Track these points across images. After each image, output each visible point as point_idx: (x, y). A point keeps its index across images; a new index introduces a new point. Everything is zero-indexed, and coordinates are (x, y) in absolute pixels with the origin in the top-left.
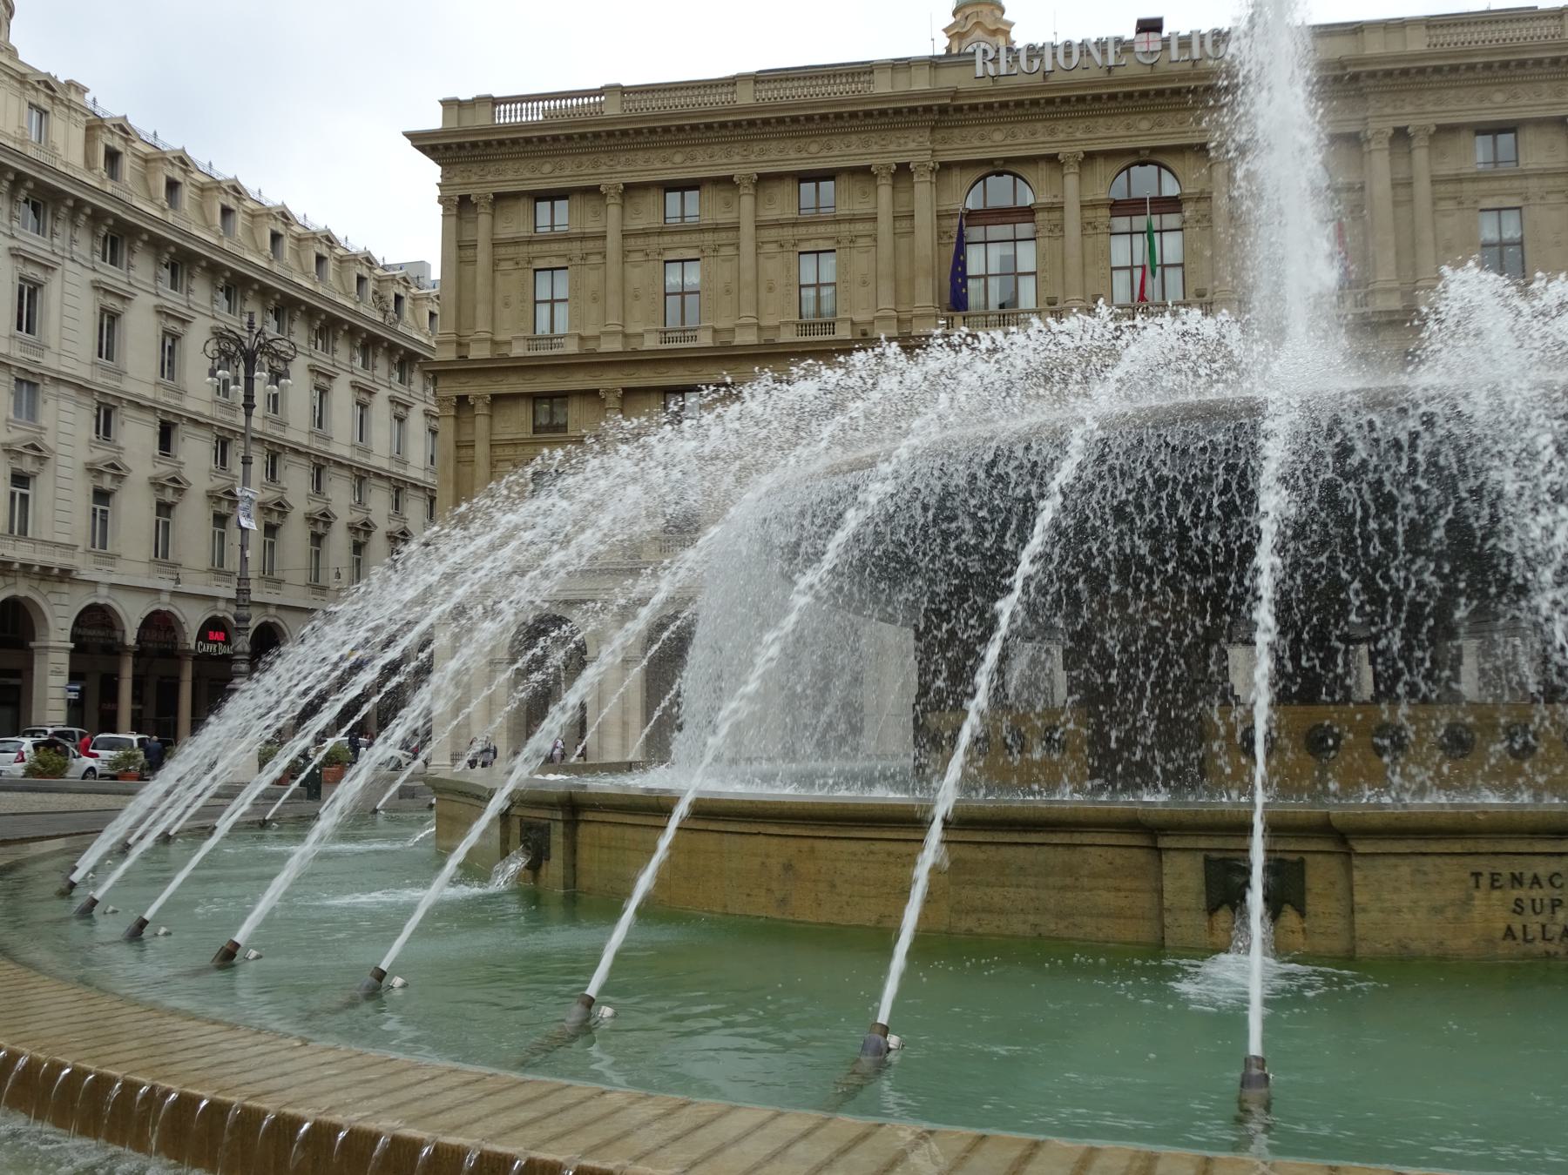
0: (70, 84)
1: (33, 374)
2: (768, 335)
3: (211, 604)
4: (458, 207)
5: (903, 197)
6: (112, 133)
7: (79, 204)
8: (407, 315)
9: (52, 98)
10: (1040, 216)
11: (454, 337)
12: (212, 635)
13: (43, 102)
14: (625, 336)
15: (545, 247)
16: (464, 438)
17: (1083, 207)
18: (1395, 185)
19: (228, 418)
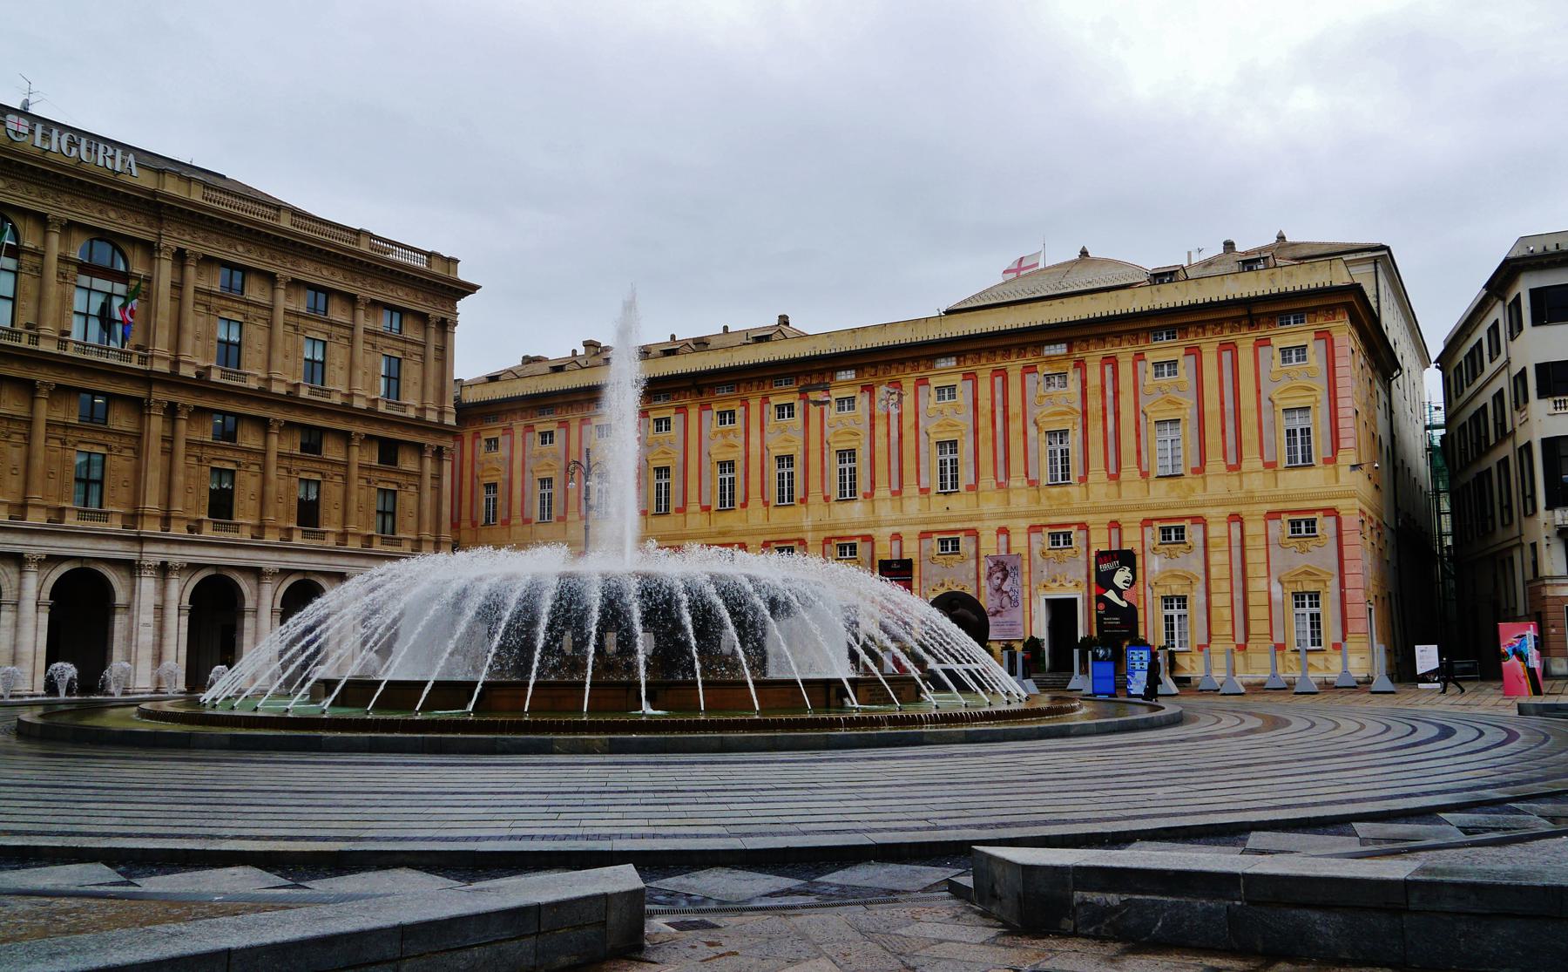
18: (173, 285)
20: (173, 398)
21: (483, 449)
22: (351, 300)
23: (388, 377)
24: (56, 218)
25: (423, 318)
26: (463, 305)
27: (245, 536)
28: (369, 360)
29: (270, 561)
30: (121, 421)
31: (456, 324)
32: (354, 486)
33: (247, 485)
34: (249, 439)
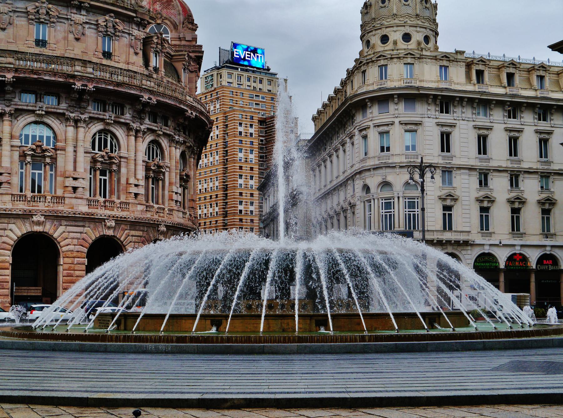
0: (457, 52)
1: (449, 168)
3: (543, 249)
6: (478, 64)
7: (462, 99)
9: (449, 61)
12: (545, 262)
13: (445, 63)
19: (546, 167)
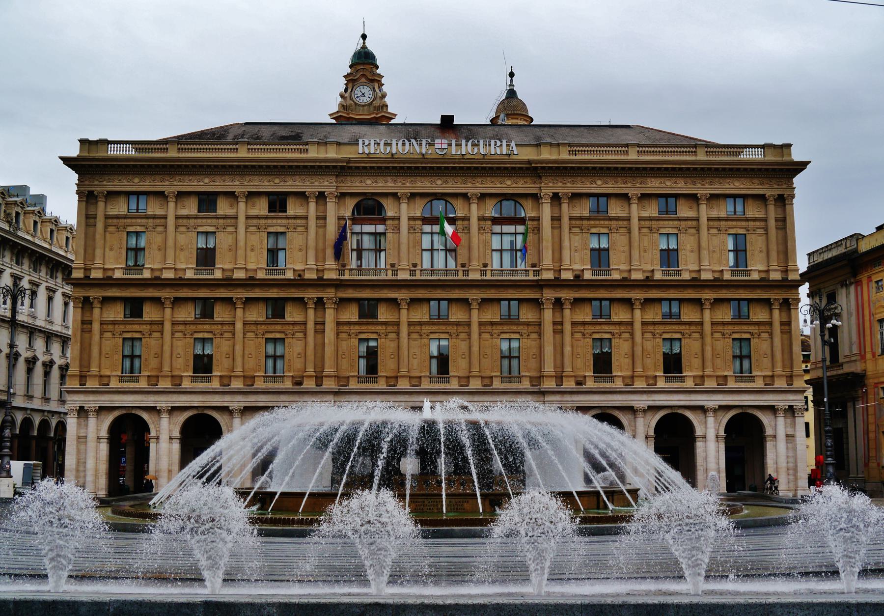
2: (251, 274)
4: (87, 197)
5: (321, 208)
8: (21, 224)
10: (388, 222)
11: (83, 266)
14: (176, 269)
15: (134, 221)
16: (86, 319)
17: (409, 219)
20: (558, 295)
21: (874, 291)
22: (693, 198)
23: (736, 251)
24: (473, 194)
25: (762, 198)
26: (797, 180)
27: (619, 384)
28: (716, 241)
29: (712, 401)
30: (527, 315)
31: (793, 196)
32: (708, 339)
33: (620, 351)
34: (620, 315)
